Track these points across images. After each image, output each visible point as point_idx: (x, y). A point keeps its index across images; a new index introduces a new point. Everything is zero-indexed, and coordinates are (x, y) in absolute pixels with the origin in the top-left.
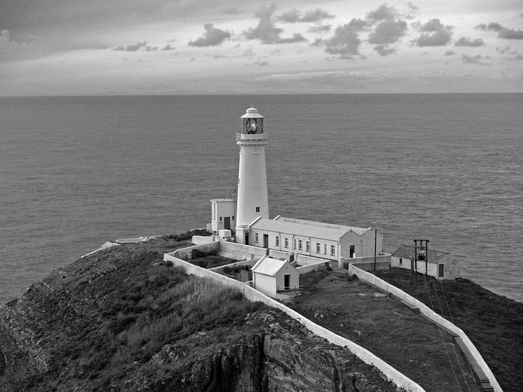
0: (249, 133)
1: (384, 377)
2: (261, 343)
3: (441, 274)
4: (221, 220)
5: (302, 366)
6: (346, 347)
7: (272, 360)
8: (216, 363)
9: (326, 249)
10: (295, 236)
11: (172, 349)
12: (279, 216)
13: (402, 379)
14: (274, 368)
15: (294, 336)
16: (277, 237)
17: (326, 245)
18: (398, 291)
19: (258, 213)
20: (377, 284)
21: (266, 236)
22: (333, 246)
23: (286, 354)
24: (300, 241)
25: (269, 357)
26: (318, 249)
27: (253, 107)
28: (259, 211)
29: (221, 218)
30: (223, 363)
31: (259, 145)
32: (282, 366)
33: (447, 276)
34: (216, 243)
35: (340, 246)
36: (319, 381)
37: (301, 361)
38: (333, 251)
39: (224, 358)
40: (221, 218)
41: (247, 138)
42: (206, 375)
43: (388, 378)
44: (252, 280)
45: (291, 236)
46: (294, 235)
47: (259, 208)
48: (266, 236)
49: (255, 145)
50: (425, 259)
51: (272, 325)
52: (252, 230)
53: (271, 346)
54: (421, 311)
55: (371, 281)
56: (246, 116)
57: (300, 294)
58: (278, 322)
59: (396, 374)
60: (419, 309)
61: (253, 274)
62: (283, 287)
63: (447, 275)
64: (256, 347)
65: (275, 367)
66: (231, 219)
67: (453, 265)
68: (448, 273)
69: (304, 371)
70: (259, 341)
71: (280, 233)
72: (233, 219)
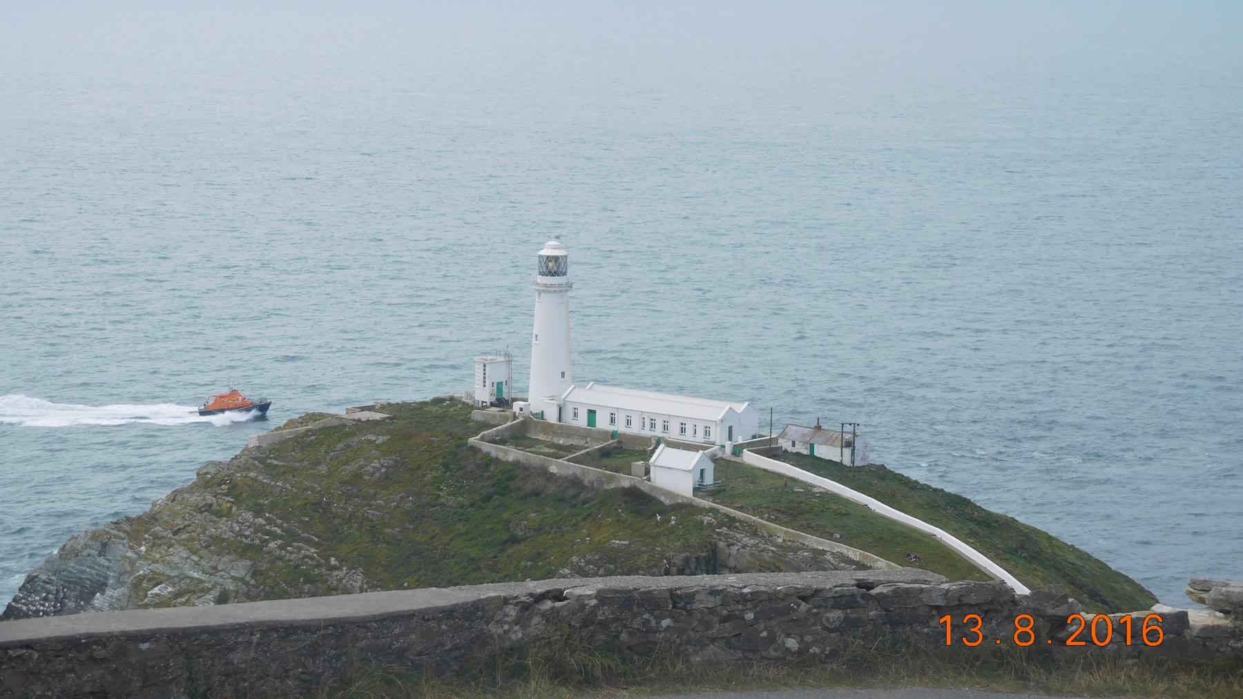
0: (553, 276)
21: (592, 413)
26: (683, 430)
35: (719, 429)
41: (545, 282)
46: (642, 412)
48: (592, 413)
49: (561, 291)
56: (545, 252)
66: (504, 384)
71: (618, 408)
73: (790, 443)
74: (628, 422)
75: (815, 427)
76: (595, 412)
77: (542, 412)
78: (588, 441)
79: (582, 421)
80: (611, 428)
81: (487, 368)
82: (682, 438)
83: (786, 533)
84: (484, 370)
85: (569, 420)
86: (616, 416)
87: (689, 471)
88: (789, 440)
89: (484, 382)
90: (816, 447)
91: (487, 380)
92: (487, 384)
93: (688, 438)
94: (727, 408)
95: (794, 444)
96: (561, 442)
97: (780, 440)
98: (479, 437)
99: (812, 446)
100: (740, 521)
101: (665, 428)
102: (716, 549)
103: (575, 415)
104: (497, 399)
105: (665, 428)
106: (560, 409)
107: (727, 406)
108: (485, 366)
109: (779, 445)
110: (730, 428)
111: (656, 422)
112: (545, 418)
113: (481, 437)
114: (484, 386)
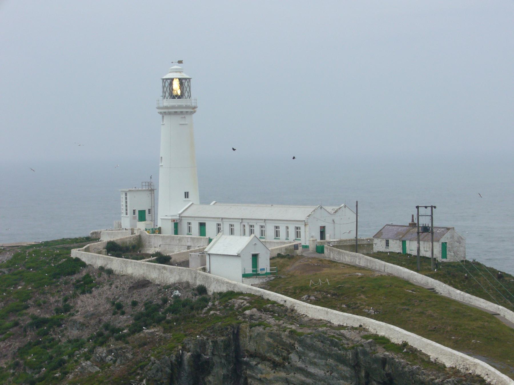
1: (424, 357)
2: (237, 335)
3: (444, 255)
4: (134, 214)
5: (300, 355)
6: (361, 326)
7: (252, 356)
8: (176, 363)
9: (288, 233)
10: (244, 221)
11: (110, 352)
12: (214, 202)
13: (452, 355)
14: (256, 365)
15: (282, 322)
16: (219, 225)
17: (287, 228)
18: (401, 270)
19: (187, 199)
20: (369, 264)
21: (202, 225)
22: (297, 228)
23: (276, 344)
24: (251, 226)
25: (247, 351)
26: (277, 234)
27: (177, 66)
28: (188, 197)
29: (134, 211)
30: (186, 362)
31: (187, 112)
32: (269, 360)
33: (450, 258)
34: (137, 236)
36: (328, 372)
37: (300, 349)
38: (298, 234)
39: (188, 355)
40: (134, 211)
42: (164, 379)
43: (431, 357)
44: (205, 265)
45: (238, 220)
46: (242, 219)
47: (188, 193)
48: (202, 225)
49: (182, 112)
51: (247, 312)
52: (182, 218)
53: (251, 336)
54: (437, 291)
55: (359, 263)
57: (273, 278)
58: (255, 307)
59: (443, 350)
60: (433, 289)
61: (207, 257)
62: (249, 270)
63: (451, 255)
64: (230, 338)
65: (259, 363)
67: (458, 244)
68: (453, 254)
69: (303, 361)
70: (234, 332)
71: (222, 219)
72: (149, 213)
73: (384, 242)
75: (410, 224)
81: (128, 197)
84: (126, 198)
86: (221, 227)
90: (407, 242)
91: (128, 208)
92: (128, 212)
95: (387, 244)
99: (404, 242)
102: (238, 331)
108: (126, 194)
111: (255, 228)
114: (127, 214)
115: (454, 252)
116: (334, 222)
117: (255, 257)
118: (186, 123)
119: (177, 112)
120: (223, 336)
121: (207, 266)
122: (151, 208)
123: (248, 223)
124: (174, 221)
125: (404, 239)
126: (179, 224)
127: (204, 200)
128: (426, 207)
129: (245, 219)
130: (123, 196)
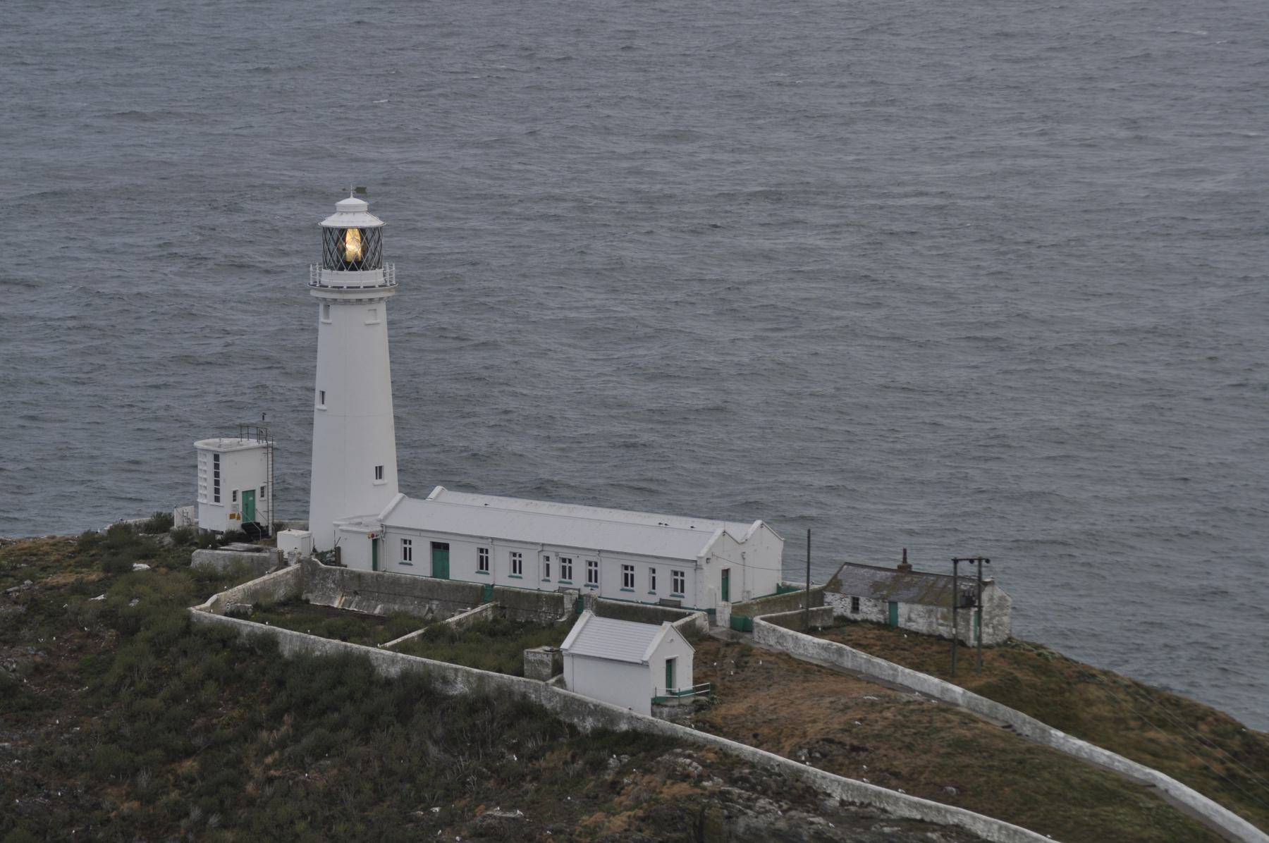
19: (379, 481)
21: (440, 548)
26: (628, 581)
27: (355, 197)
28: (380, 478)
38: (679, 586)
45: (533, 547)
47: (381, 467)
48: (440, 548)
49: (371, 300)
50: (977, 604)
56: (332, 221)
61: (567, 664)
62: (662, 692)
63: (988, 634)
68: (991, 631)
70: (694, 823)
71: (493, 539)
72: (262, 496)
73: (848, 602)
74: (517, 567)
76: (446, 547)
77: (338, 550)
78: (434, 607)
79: (421, 567)
80: (481, 580)
81: (221, 463)
82: (626, 596)
83: (846, 787)
85: (392, 564)
87: (644, 665)
88: (846, 595)
89: (217, 491)
92: (222, 495)
93: (640, 595)
94: (719, 532)
95: (855, 607)
96: (377, 611)
97: (829, 597)
98: (208, 603)
99: (894, 604)
100: (752, 766)
101: (593, 576)
102: (701, 823)
103: (407, 554)
104: (243, 526)
105: (593, 576)
106: (375, 542)
107: (718, 528)
108: (217, 457)
109: (826, 607)
110: (726, 573)
112: (344, 561)
113: (213, 605)
114: (217, 499)
115: (993, 627)
116: (744, 559)
117: (670, 663)
118: (378, 321)
119: (361, 300)
120: (675, 830)
121: (567, 674)
122: (266, 484)
123: (557, 555)
124: (373, 536)
125: (892, 598)
126: (380, 543)
127: (414, 485)
128: (972, 561)
129: (549, 545)
130: (210, 460)
